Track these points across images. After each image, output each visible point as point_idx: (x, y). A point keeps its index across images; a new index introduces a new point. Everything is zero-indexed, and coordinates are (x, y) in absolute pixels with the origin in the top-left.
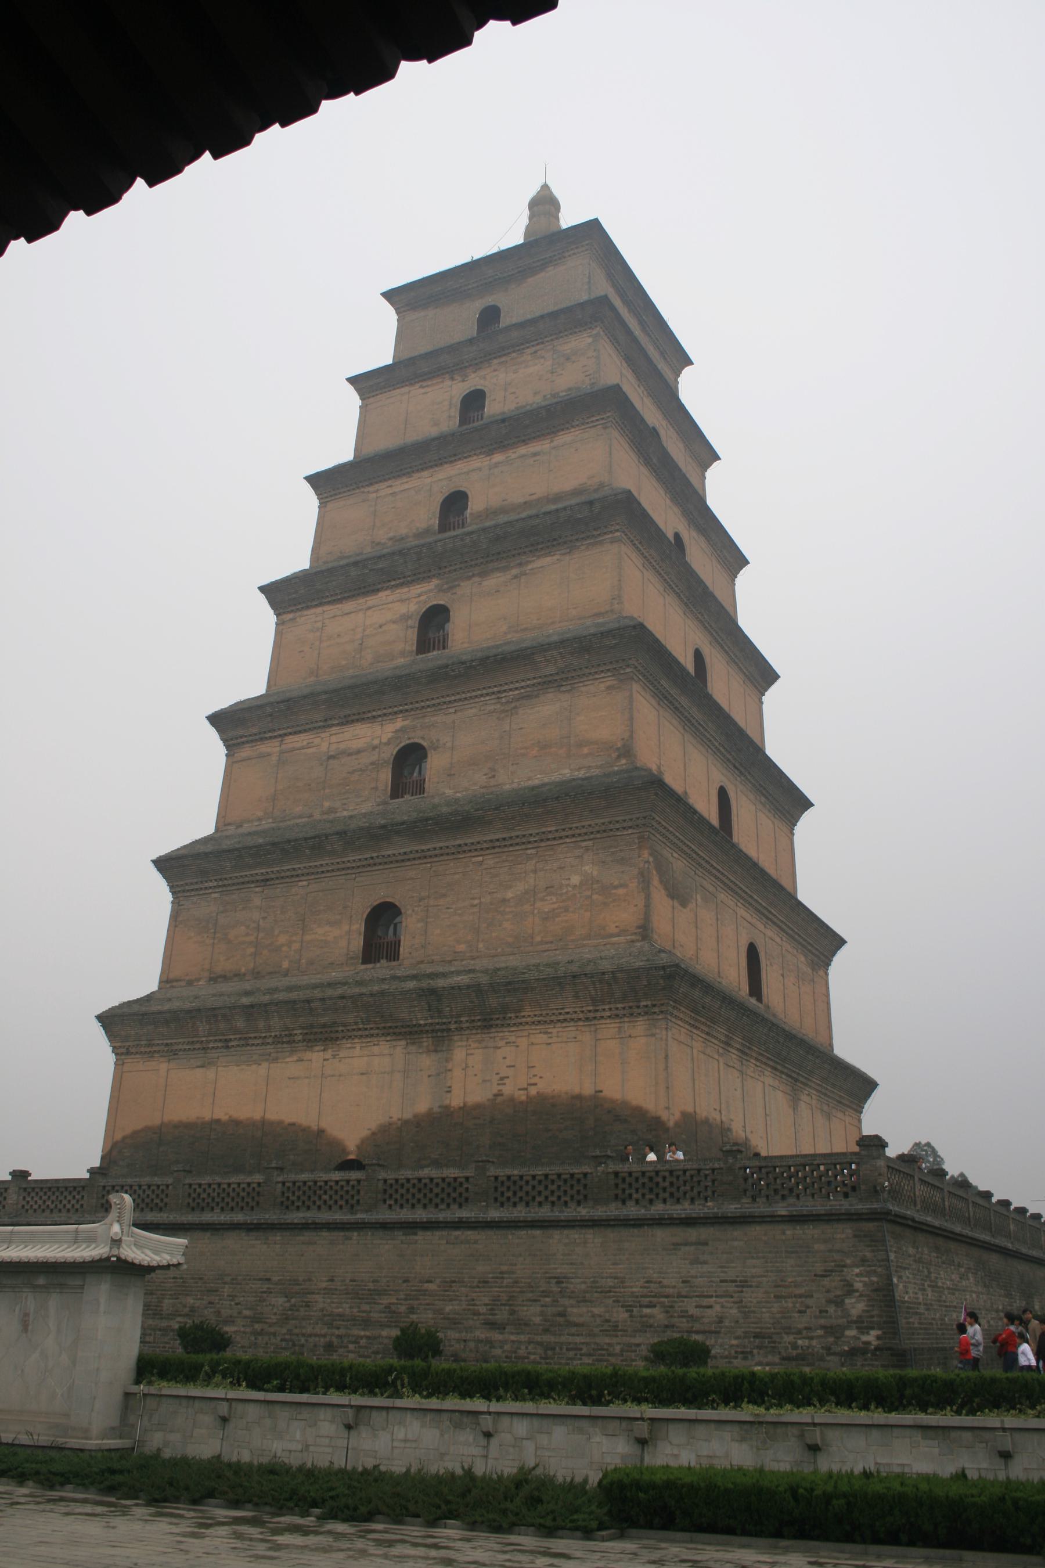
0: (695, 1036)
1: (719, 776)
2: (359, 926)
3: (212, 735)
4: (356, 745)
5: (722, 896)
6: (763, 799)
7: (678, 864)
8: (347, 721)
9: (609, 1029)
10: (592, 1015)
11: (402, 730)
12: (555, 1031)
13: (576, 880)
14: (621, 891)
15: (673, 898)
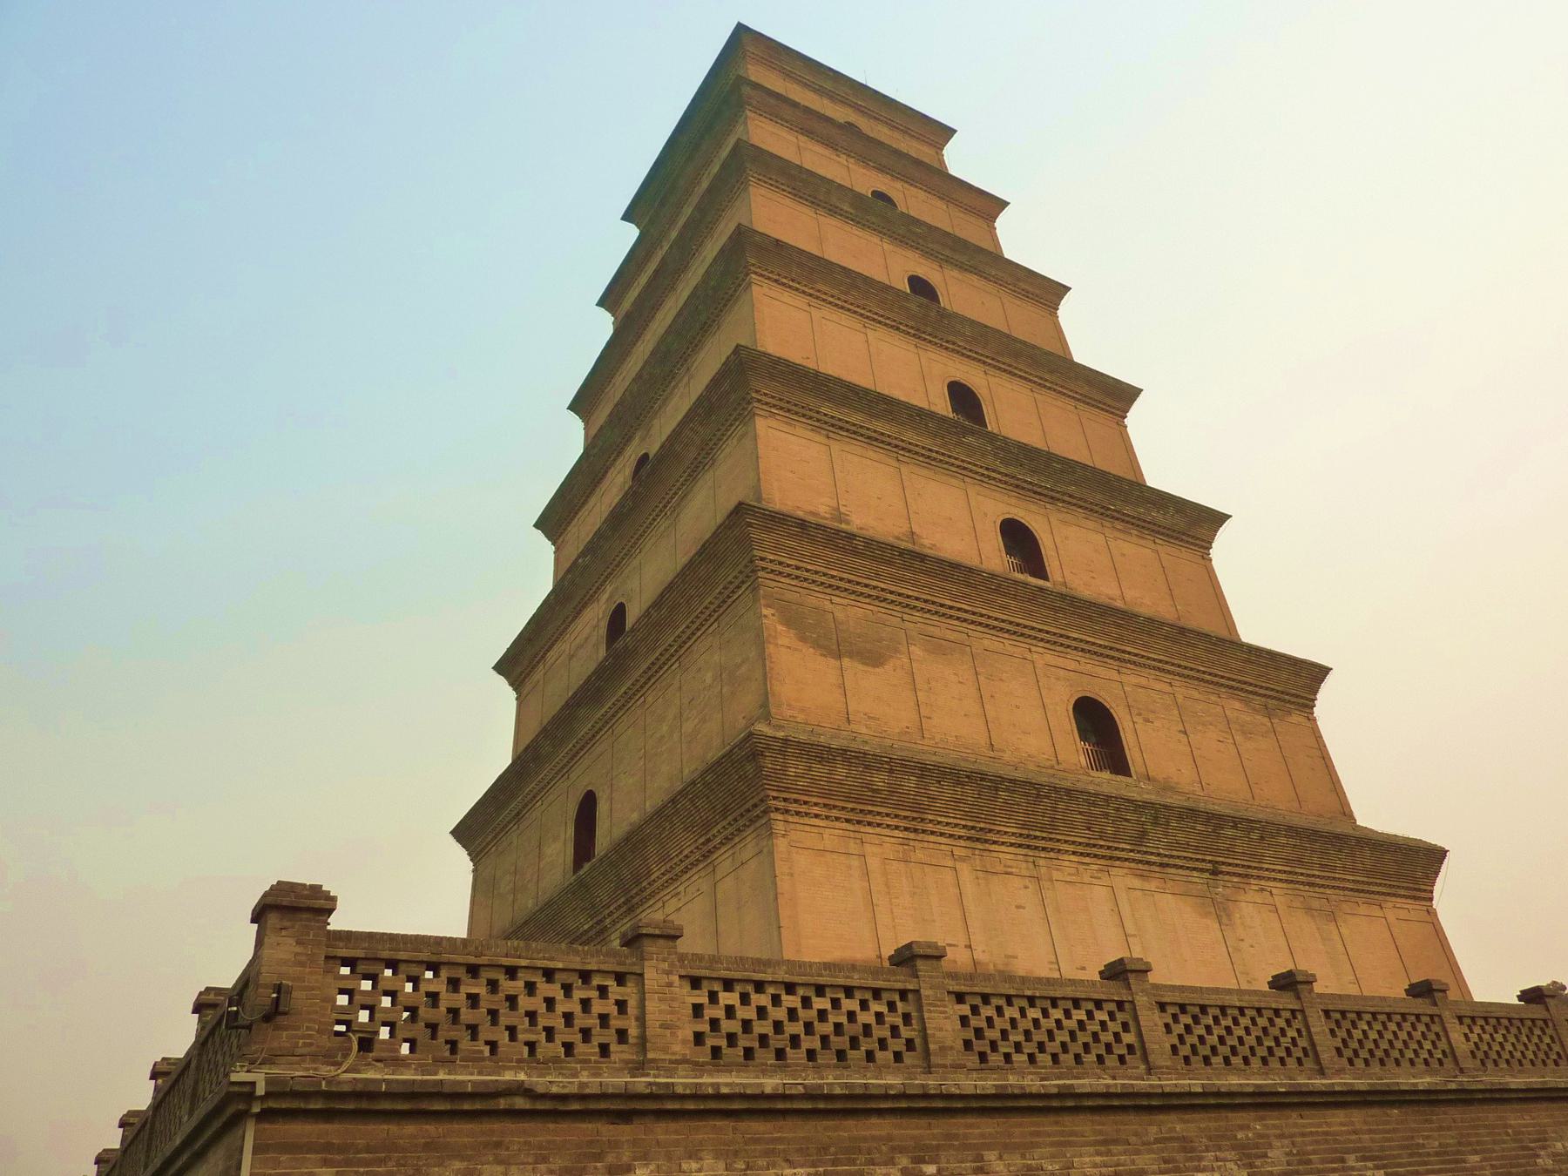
0: (866, 838)
1: (997, 506)
2: (571, 831)
3: (502, 682)
4: (587, 630)
5: (990, 642)
6: (1119, 525)
7: (849, 613)
8: (578, 613)
9: (724, 860)
10: (705, 848)
11: (611, 596)
12: (681, 889)
13: (709, 677)
14: (743, 669)
15: (839, 656)
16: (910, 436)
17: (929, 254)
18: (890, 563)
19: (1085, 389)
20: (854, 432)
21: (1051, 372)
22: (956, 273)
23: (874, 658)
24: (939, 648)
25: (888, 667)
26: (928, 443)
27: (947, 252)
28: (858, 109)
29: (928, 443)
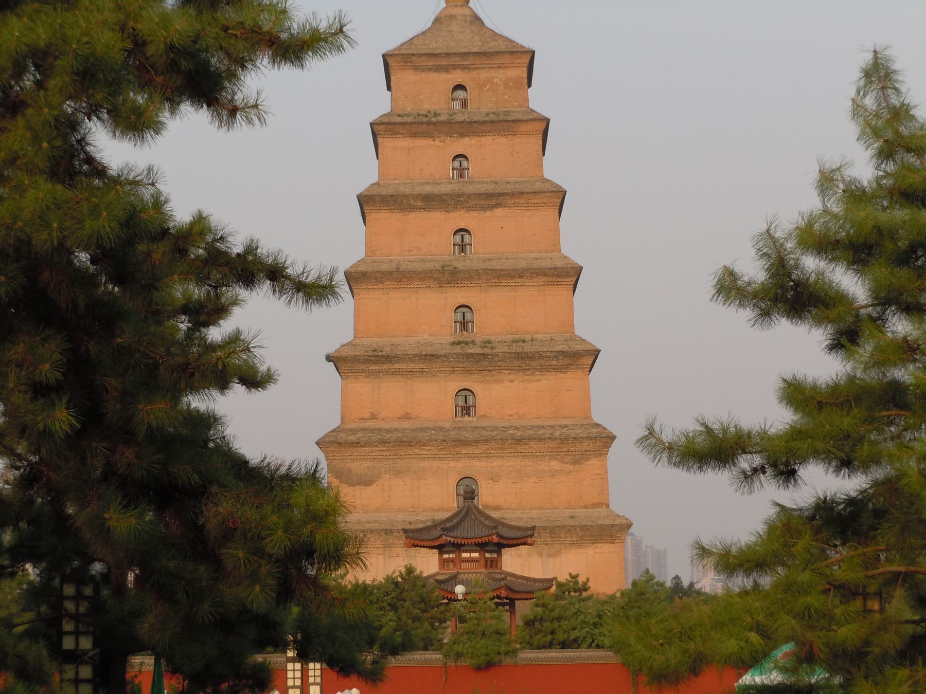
6: (530, 372)
16: (412, 366)
17: (469, 209)
18: (376, 446)
19: (544, 279)
20: (386, 372)
21: (521, 277)
22: (488, 213)
23: (369, 483)
24: (398, 473)
25: (374, 485)
26: (420, 366)
27: (482, 202)
28: (464, 68)
29: (420, 366)
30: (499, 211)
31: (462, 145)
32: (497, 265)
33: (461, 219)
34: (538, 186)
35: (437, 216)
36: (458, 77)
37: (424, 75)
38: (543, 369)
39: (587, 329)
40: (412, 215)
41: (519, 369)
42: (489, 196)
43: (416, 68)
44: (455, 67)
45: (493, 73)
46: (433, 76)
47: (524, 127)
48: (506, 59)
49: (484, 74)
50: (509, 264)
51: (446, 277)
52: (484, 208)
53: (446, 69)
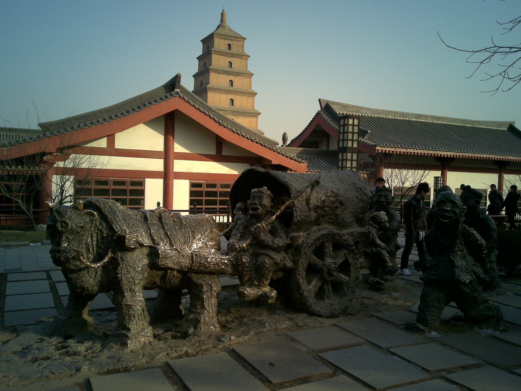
28: (231, 40)
30: (239, 77)
31: (231, 59)
32: (239, 90)
33: (232, 78)
34: (247, 72)
35: (225, 76)
36: (229, 42)
37: (221, 40)
38: (249, 116)
39: (257, 108)
40: (220, 75)
41: (244, 116)
42: (238, 73)
43: (220, 38)
44: (229, 39)
45: (237, 42)
46: (224, 40)
47: (244, 57)
48: (240, 39)
49: (235, 42)
50: (242, 90)
51: (228, 92)
52: (236, 76)
53: (226, 39)
